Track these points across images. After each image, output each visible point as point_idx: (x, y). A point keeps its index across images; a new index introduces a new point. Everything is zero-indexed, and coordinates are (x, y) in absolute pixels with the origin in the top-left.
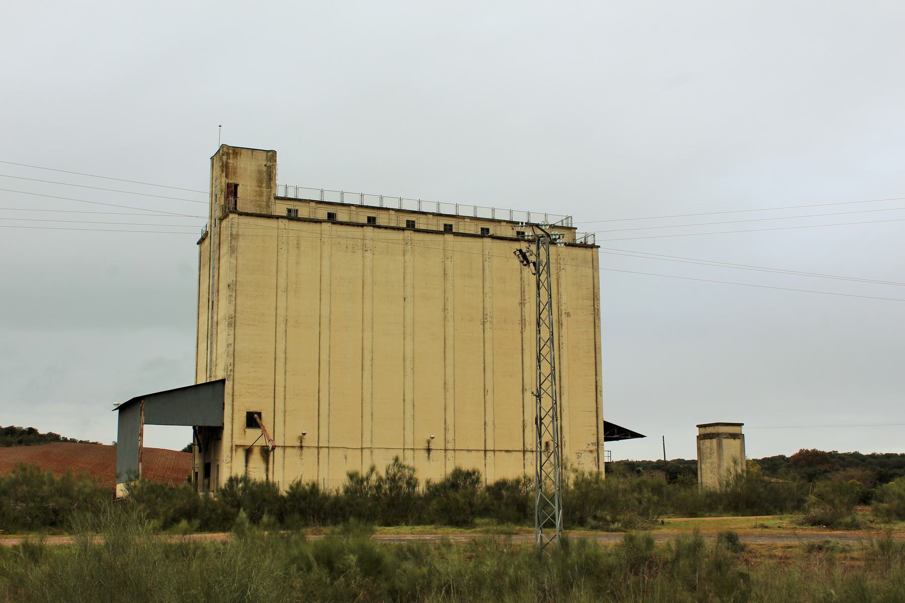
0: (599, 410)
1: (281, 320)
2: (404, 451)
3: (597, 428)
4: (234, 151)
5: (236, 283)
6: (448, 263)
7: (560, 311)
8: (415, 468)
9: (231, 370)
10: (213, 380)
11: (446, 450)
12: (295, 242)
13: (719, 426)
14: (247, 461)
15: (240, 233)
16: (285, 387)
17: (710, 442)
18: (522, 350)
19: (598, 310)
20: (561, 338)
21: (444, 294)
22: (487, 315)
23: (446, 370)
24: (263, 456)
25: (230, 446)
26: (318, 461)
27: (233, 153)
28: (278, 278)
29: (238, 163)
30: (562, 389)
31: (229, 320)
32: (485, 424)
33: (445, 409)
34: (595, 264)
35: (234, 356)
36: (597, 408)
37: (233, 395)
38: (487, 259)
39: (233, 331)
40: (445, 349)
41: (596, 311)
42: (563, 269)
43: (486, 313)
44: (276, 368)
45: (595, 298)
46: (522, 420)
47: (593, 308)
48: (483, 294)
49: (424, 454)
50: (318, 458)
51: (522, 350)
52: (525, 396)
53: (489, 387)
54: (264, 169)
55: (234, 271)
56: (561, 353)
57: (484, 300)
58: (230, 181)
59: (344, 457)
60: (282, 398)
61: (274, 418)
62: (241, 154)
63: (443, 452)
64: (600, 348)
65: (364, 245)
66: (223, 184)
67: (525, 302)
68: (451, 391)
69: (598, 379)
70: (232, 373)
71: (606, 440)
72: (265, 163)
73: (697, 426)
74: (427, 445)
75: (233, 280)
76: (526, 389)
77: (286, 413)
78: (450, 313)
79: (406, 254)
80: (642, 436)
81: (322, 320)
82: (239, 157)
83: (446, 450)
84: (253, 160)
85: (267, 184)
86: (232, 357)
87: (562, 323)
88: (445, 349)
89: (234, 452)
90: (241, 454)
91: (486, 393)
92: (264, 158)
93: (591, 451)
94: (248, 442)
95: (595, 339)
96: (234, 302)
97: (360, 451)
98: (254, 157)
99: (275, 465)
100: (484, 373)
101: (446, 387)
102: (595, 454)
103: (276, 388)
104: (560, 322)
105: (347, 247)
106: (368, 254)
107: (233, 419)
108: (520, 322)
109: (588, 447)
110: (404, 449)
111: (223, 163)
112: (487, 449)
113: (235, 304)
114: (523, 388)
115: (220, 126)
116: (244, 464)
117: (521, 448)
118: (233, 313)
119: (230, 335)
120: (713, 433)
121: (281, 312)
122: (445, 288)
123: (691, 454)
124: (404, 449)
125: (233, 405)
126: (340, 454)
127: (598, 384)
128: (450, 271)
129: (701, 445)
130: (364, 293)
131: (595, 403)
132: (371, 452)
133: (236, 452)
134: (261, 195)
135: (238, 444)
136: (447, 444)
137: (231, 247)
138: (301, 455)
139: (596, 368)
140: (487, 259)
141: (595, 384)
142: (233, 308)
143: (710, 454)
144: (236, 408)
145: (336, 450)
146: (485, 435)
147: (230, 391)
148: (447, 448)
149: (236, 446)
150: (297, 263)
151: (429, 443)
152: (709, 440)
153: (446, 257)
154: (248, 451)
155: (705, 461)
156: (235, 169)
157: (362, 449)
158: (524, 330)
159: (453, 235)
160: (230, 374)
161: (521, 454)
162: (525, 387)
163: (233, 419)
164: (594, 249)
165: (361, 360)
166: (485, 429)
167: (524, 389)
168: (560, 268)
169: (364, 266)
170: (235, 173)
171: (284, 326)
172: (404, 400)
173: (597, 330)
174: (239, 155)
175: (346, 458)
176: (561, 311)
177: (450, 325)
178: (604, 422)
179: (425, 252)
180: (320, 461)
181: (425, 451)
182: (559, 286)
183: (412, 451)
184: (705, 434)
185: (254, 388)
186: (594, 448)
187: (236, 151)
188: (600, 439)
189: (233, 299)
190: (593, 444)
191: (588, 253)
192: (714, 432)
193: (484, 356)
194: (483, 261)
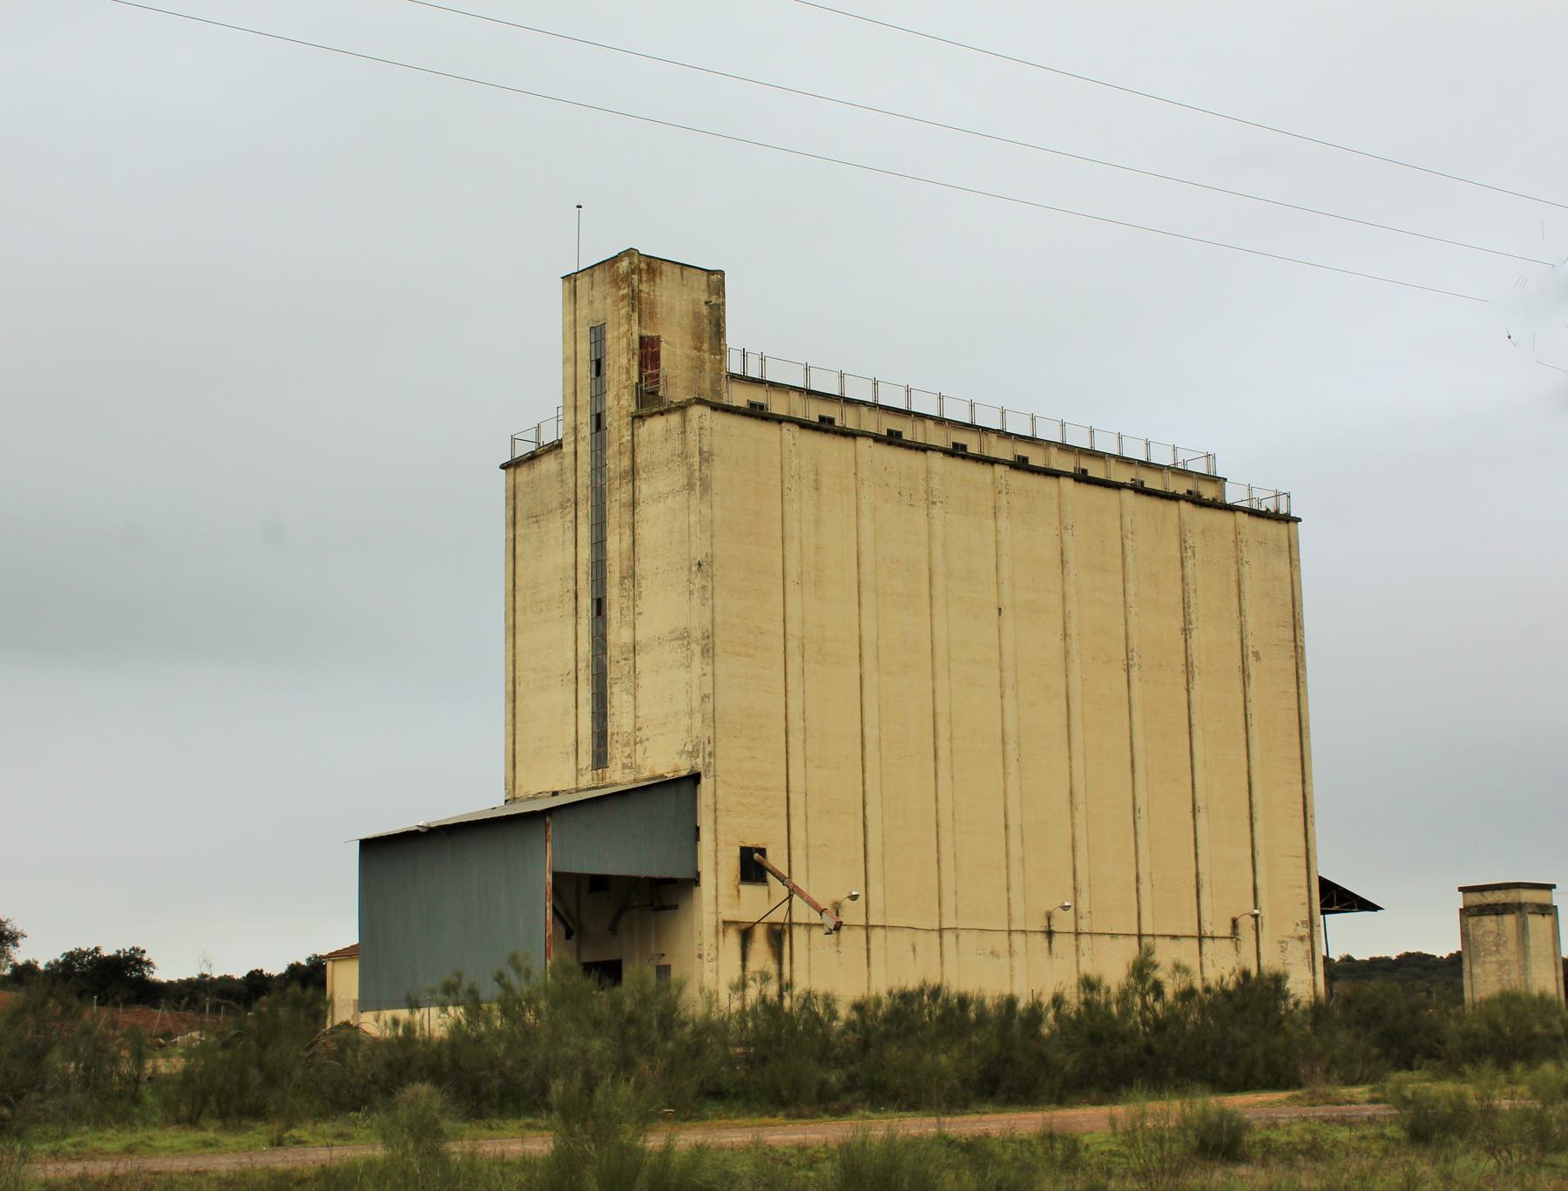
0: (1311, 853)
1: (793, 645)
2: (1009, 935)
3: (1310, 891)
4: (648, 265)
5: (711, 561)
6: (1067, 537)
7: (1245, 649)
8: (1088, 973)
9: (710, 754)
10: (619, 776)
11: (1077, 934)
12: (812, 476)
13: (1520, 890)
14: (744, 958)
15: (716, 451)
17: (1497, 922)
18: (1190, 726)
19: (1303, 648)
20: (1248, 704)
21: (1064, 603)
22: (1133, 650)
23: (1074, 765)
24: (771, 946)
25: (715, 924)
26: (868, 957)
27: (648, 270)
28: (786, 553)
29: (658, 294)
30: (1255, 809)
31: (704, 642)
34: (1294, 556)
35: (714, 721)
37: (715, 810)
38: (1129, 535)
39: (710, 667)
40: (1068, 720)
41: (1299, 651)
42: (1247, 562)
43: (1130, 646)
44: (790, 750)
47: (1292, 644)
49: (1041, 940)
50: (868, 950)
51: (1190, 726)
52: (1198, 822)
53: (1141, 803)
54: (705, 310)
55: (708, 534)
56: (1250, 735)
57: (1126, 620)
58: (646, 333)
59: (911, 949)
60: (803, 817)
62: (661, 274)
63: (1072, 936)
64: (1307, 727)
65: (929, 492)
66: (636, 338)
68: (1082, 808)
70: (712, 760)
71: (1323, 913)
72: (704, 297)
73: (1461, 889)
74: (1047, 924)
78: (1074, 646)
79: (998, 515)
80: (1374, 908)
81: (866, 648)
82: (658, 280)
83: (1077, 934)
84: (685, 289)
85: (711, 344)
86: (712, 724)
87: (1249, 674)
88: (1068, 720)
89: (721, 935)
90: (733, 940)
91: (1138, 815)
92: (704, 286)
93: (1301, 939)
94: (748, 915)
95: (1299, 709)
97: (936, 935)
98: (685, 282)
100: (1133, 773)
101: (1074, 801)
102: (1307, 945)
103: (791, 795)
104: (1247, 673)
105: (900, 493)
106: (937, 511)
107: (716, 863)
108: (1184, 668)
109: (1296, 930)
110: (1010, 932)
111: (633, 291)
113: (713, 605)
115: (579, 207)
117: (1195, 932)
118: (710, 627)
119: (704, 675)
120: (1504, 904)
121: (793, 628)
122: (1063, 591)
123: (1442, 942)
125: (716, 830)
126: (904, 938)
127: (1308, 800)
128: (1071, 556)
129: (1470, 927)
131: (1304, 839)
132: (957, 937)
133: (724, 936)
135: (727, 919)
137: (701, 479)
138: (838, 944)
139: (1303, 768)
140: (1129, 535)
141: (1301, 800)
142: (709, 614)
143: (1497, 945)
144: (721, 838)
145: (897, 933)
146: (1138, 902)
147: (710, 801)
148: (1079, 931)
149: (725, 922)
150: (817, 522)
151: (1049, 919)
152: (1494, 918)
153: (1063, 526)
154: (746, 934)
155: (1481, 959)
156: (652, 304)
157: (941, 930)
160: (710, 763)
161: (1196, 942)
163: (716, 863)
164: (1291, 524)
165: (932, 739)
166: (1138, 890)
167: (1197, 808)
168: (1242, 559)
169: (930, 536)
170: (652, 315)
171: (801, 659)
172: (1006, 827)
174: (658, 275)
175: (914, 951)
176: (1247, 648)
177: (1076, 668)
178: (1320, 878)
179: (1029, 512)
181: (1044, 936)
182: (1242, 598)
183: (1023, 935)
184: (1480, 905)
185: (751, 794)
186: (1305, 931)
187: (652, 266)
189: (708, 595)
190: (1303, 923)
191: (1282, 528)
192: (1508, 900)
193: (1131, 738)
194: (1122, 539)
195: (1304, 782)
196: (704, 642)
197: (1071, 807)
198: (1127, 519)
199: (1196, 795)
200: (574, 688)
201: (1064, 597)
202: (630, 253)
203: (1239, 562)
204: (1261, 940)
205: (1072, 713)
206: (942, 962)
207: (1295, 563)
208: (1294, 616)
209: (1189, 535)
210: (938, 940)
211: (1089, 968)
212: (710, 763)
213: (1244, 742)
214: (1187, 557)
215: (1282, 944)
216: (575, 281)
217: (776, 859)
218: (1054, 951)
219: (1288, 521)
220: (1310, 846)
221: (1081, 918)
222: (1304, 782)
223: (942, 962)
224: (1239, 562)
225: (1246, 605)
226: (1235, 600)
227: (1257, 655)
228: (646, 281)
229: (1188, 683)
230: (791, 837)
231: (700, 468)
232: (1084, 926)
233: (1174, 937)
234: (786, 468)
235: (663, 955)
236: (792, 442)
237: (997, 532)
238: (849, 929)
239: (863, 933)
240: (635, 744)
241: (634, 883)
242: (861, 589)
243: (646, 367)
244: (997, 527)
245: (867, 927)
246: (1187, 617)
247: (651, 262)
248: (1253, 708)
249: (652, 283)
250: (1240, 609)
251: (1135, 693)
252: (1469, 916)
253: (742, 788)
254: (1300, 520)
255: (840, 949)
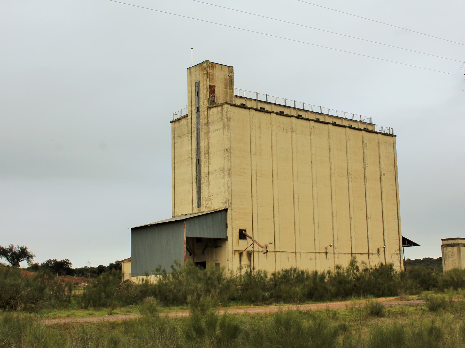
2: (315, 254)
3: (399, 241)
4: (212, 65)
5: (230, 148)
6: (331, 141)
7: (381, 172)
8: (338, 264)
9: (230, 203)
10: (204, 210)
11: (334, 253)
12: (258, 124)
13: (458, 240)
14: (240, 261)
16: (257, 214)
17: (452, 249)
18: (366, 194)
19: (397, 172)
20: (382, 188)
22: (349, 173)
24: (248, 257)
26: (275, 260)
27: (212, 66)
28: (252, 146)
29: (214, 73)
30: (384, 218)
31: (228, 172)
32: (351, 238)
33: (333, 229)
34: (394, 146)
36: (399, 229)
37: (232, 219)
38: (348, 140)
39: (230, 179)
41: (396, 173)
43: (349, 172)
44: (253, 202)
45: (395, 165)
46: (367, 236)
47: (394, 171)
48: (347, 161)
49: (324, 255)
50: (275, 258)
51: (366, 194)
52: (368, 221)
53: (352, 216)
54: (228, 77)
55: (229, 141)
56: (382, 197)
57: (347, 165)
58: (211, 84)
61: (253, 233)
62: (215, 67)
63: (333, 254)
64: (399, 194)
65: (291, 128)
67: (366, 166)
68: (335, 218)
69: (399, 212)
70: (231, 205)
71: (403, 247)
72: (228, 74)
73: (442, 240)
74: (325, 250)
75: (229, 147)
76: (368, 217)
77: (259, 231)
78: (333, 172)
80: (417, 245)
82: (214, 69)
83: (334, 253)
84: (222, 71)
85: (230, 87)
86: (231, 195)
87: (382, 180)
90: (237, 255)
91: (351, 220)
92: (227, 71)
93: (397, 254)
95: (396, 189)
96: (230, 160)
97: (294, 254)
98: (222, 69)
99: (254, 263)
100: (350, 208)
101: (333, 216)
103: (253, 215)
104: (381, 179)
105: (283, 129)
106: (294, 134)
108: (364, 178)
109: (396, 252)
110: (315, 253)
111: (207, 72)
112: (353, 252)
113: (231, 161)
114: (367, 217)
115: (192, 48)
116: (239, 262)
117: (367, 252)
118: (230, 167)
120: (454, 244)
121: (254, 167)
123: (436, 254)
124: (315, 253)
126: (285, 255)
128: (332, 146)
130: (293, 157)
131: (397, 226)
132: (300, 254)
134: (226, 94)
135: (236, 249)
136: (335, 250)
137: (227, 125)
138: (267, 256)
139: (397, 206)
140: (348, 140)
141: (397, 215)
142: (230, 164)
143: (452, 255)
146: (351, 244)
147: (231, 217)
149: (235, 251)
150: (260, 137)
152: (451, 248)
154: (241, 254)
155: (447, 259)
156: (213, 76)
157: (296, 252)
158: (366, 183)
159: (332, 125)
160: (230, 206)
161: (367, 255)
162: (368, 216)
164: (394, 137)
165: (293, 199)
166: (351, 241)
167: (368, 218)
170: (213, 79)
171: (256, 176)
172: (314, 223)
173: (397, 184)
174: (214, 68)
177: (333, 178)
178: (402, 237)
180: (276, 260)
181: (325, 254)
182: (380, 158)
184: (447, 244)
186: (398, 252)
187: (213, 65)
188: (401, 247)
190: (398, 249)
191: (391, 138)
192: (455, 243)
195: (398, 210)
196: (228, 172)
197: (332, 217)
198: (347, 136)
199: (367, 214)
200: (192, 185)
201: (330, 158)
202: (206, 61)
203: (379, 148)
204: (386, 254)
205: (332, 191)
206: (296, 261)
207: (395, 148)
208: (395, 163)
209: (365, 140)
210: (295, 255)
211: (338, 262)
212: (230, 206)
213: (381, 199)
214: (364, 147)
215: (392, 256)
216: (191, 69)
217: (249, 233)
218: (328, 258)
219: (393, 136)
220: (399, 228)
221: (335, 249)
222: (398, 210)
223: (296, 261)
224: (379, 148)
225: (381, 160)
226: (378, 159)
227: (384, 174)
228: (211, 69)
229: (365, 182)
230: (253, 227)
231: (227, 122)
232: (336, 251)
233: (361, 254)
234: (251, 122)
235: (217, 260)
236: (253, 115)
237: (311, 140)
238: (270, 252)
239: (274, 254)
240: (209, 200)
241: (209, 240)
242: (273, 156)
243: (211, 94)
244: (311, 139)
245: (275, 252)
246: (365, 164)
247: (212, 64)
248: (383, 189)
249: (213, 70)
250: (379, 161)
251: (350, 185)
252: (444, 247)
253: (239, 213)
254: (396, 136)
255: (267, 258)
